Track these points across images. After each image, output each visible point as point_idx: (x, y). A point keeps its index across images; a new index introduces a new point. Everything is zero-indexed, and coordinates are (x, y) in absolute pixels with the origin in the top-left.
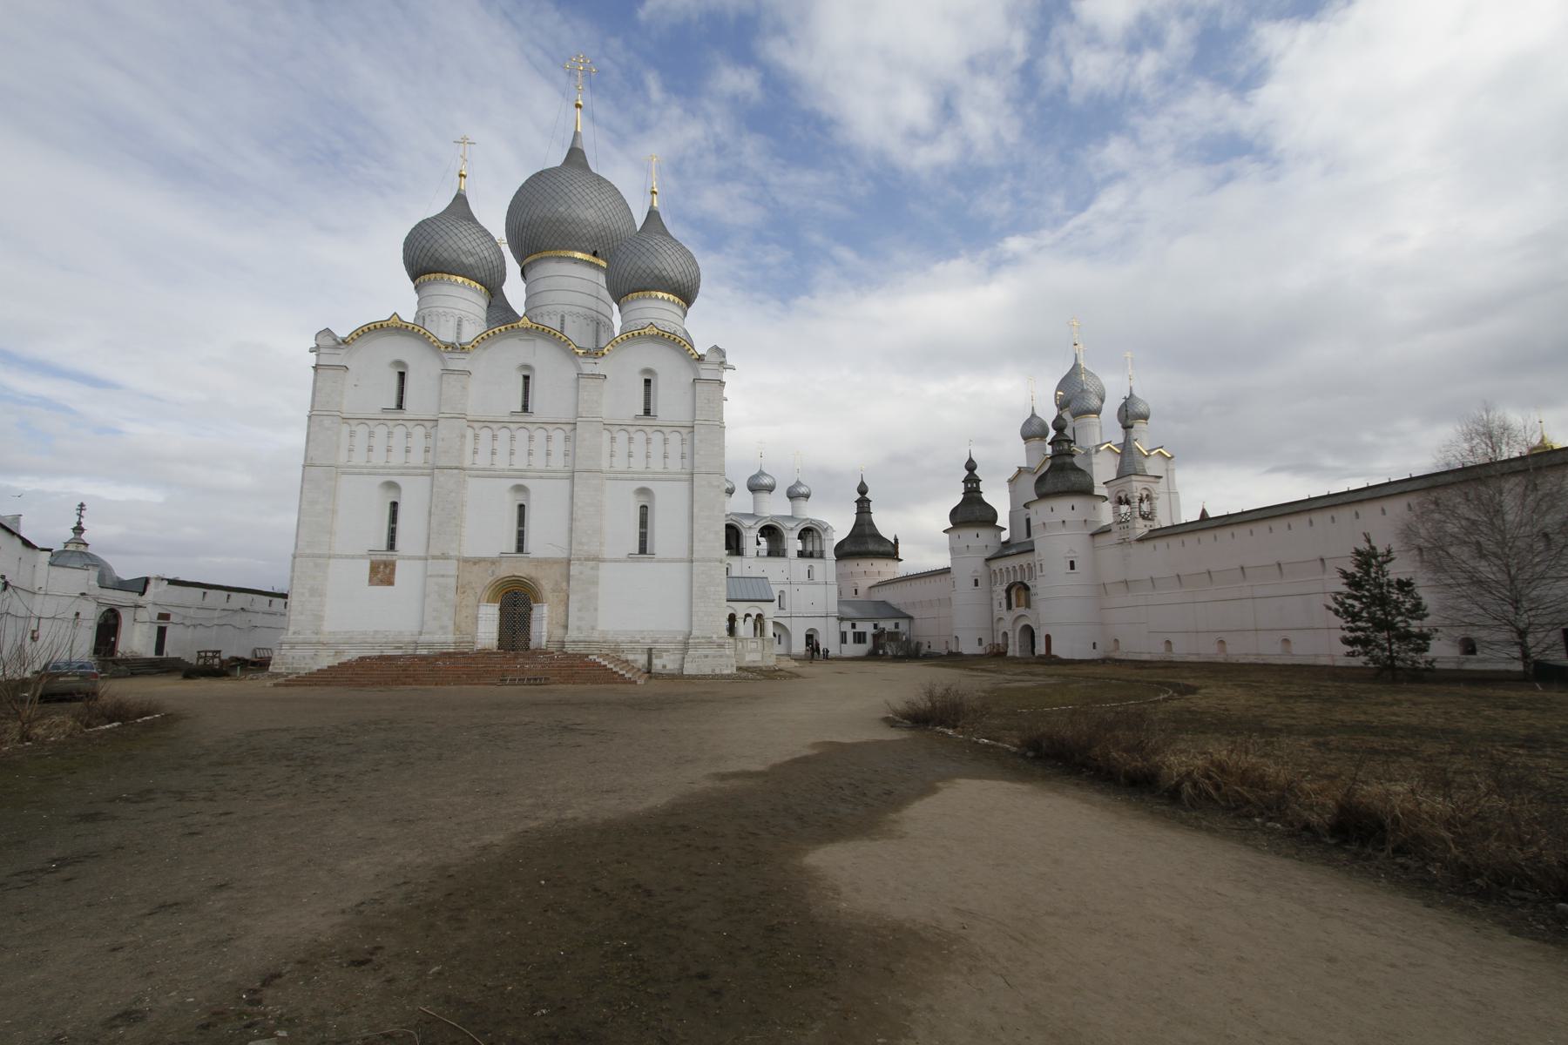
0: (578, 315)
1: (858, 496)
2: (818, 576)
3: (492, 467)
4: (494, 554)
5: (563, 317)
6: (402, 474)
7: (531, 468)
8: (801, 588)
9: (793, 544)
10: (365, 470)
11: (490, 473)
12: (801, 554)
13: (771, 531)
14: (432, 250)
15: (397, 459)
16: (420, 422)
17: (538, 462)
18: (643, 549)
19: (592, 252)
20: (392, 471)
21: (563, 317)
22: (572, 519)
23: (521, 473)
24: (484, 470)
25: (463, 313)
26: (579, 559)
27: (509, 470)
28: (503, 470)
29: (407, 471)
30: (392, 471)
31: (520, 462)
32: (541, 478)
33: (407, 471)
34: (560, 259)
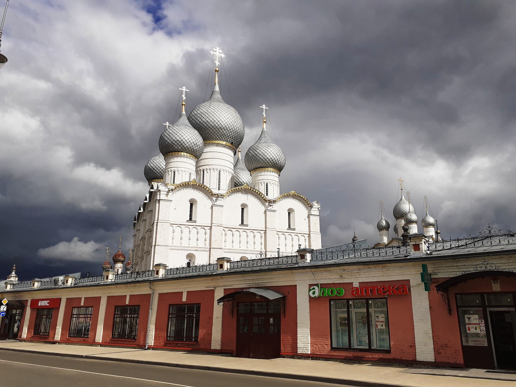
5: (220, 171)
6: (197, 250)
7: (249, 249)
21: (220, 171)
28: (237, 250)
34: (218, 145)
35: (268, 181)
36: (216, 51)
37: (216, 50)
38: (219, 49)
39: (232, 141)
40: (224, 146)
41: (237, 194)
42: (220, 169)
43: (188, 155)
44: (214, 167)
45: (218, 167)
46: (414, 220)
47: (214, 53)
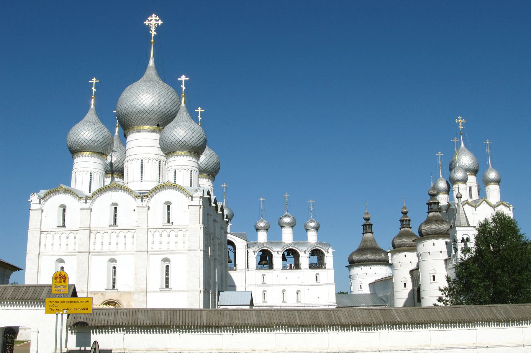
0: (149, 159)
1: (364, 222)
2: (321, 279)
3: (102, 251)
4: (103, 289)
5: (142, 160)
6: (65, 255)
8: (309, 287)
9: (305, 259)
10: (51, 254)
11: (100, 254)
12: (311, 266)
13: (294, 252)
14: (79, 142)
15: (64, 248)
16: (71, 231)
17: (121, 247)
18: (167, 286)
19: (156, 125)
20: (61, 254)
21: (142, 160)
22: (136, 274)
23: (114, 253)
24: (97, 252)
25: (93, 169)
26: (137, 292)
27: (108, 252)
29: (68, 254)
30: (61, 254)
31: (113, 248)
32: (121, 255)
33: (68, 254)
34: (141, 131)
35: (176, 167)
36: (151, 20)
37: (152, 18)
38: (155, 16)
39: (157, 124)
40: (148, 131)
41: (108, 192)
42: (142, 159)
43: (88, 153)
44: (136, 157)
45: (140, 157)
46: (459, 179)
47: (149, 23)
